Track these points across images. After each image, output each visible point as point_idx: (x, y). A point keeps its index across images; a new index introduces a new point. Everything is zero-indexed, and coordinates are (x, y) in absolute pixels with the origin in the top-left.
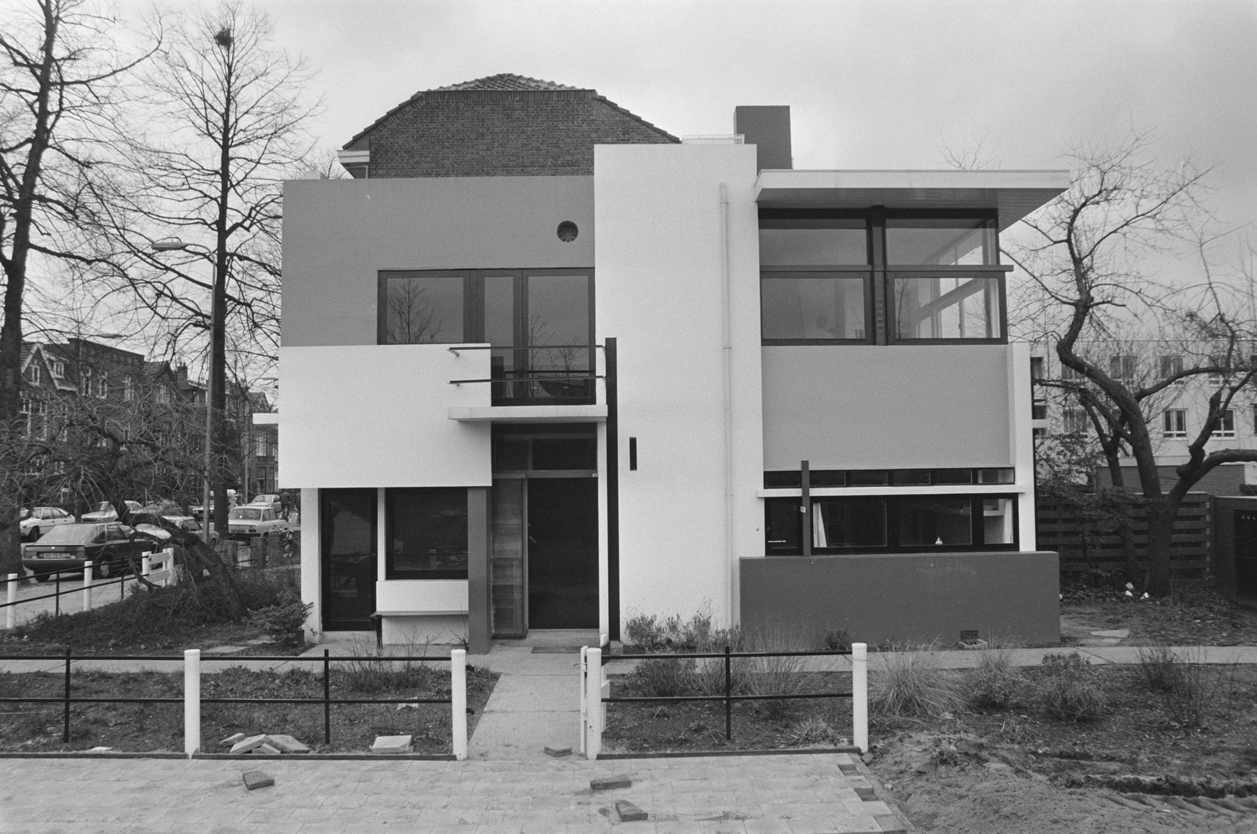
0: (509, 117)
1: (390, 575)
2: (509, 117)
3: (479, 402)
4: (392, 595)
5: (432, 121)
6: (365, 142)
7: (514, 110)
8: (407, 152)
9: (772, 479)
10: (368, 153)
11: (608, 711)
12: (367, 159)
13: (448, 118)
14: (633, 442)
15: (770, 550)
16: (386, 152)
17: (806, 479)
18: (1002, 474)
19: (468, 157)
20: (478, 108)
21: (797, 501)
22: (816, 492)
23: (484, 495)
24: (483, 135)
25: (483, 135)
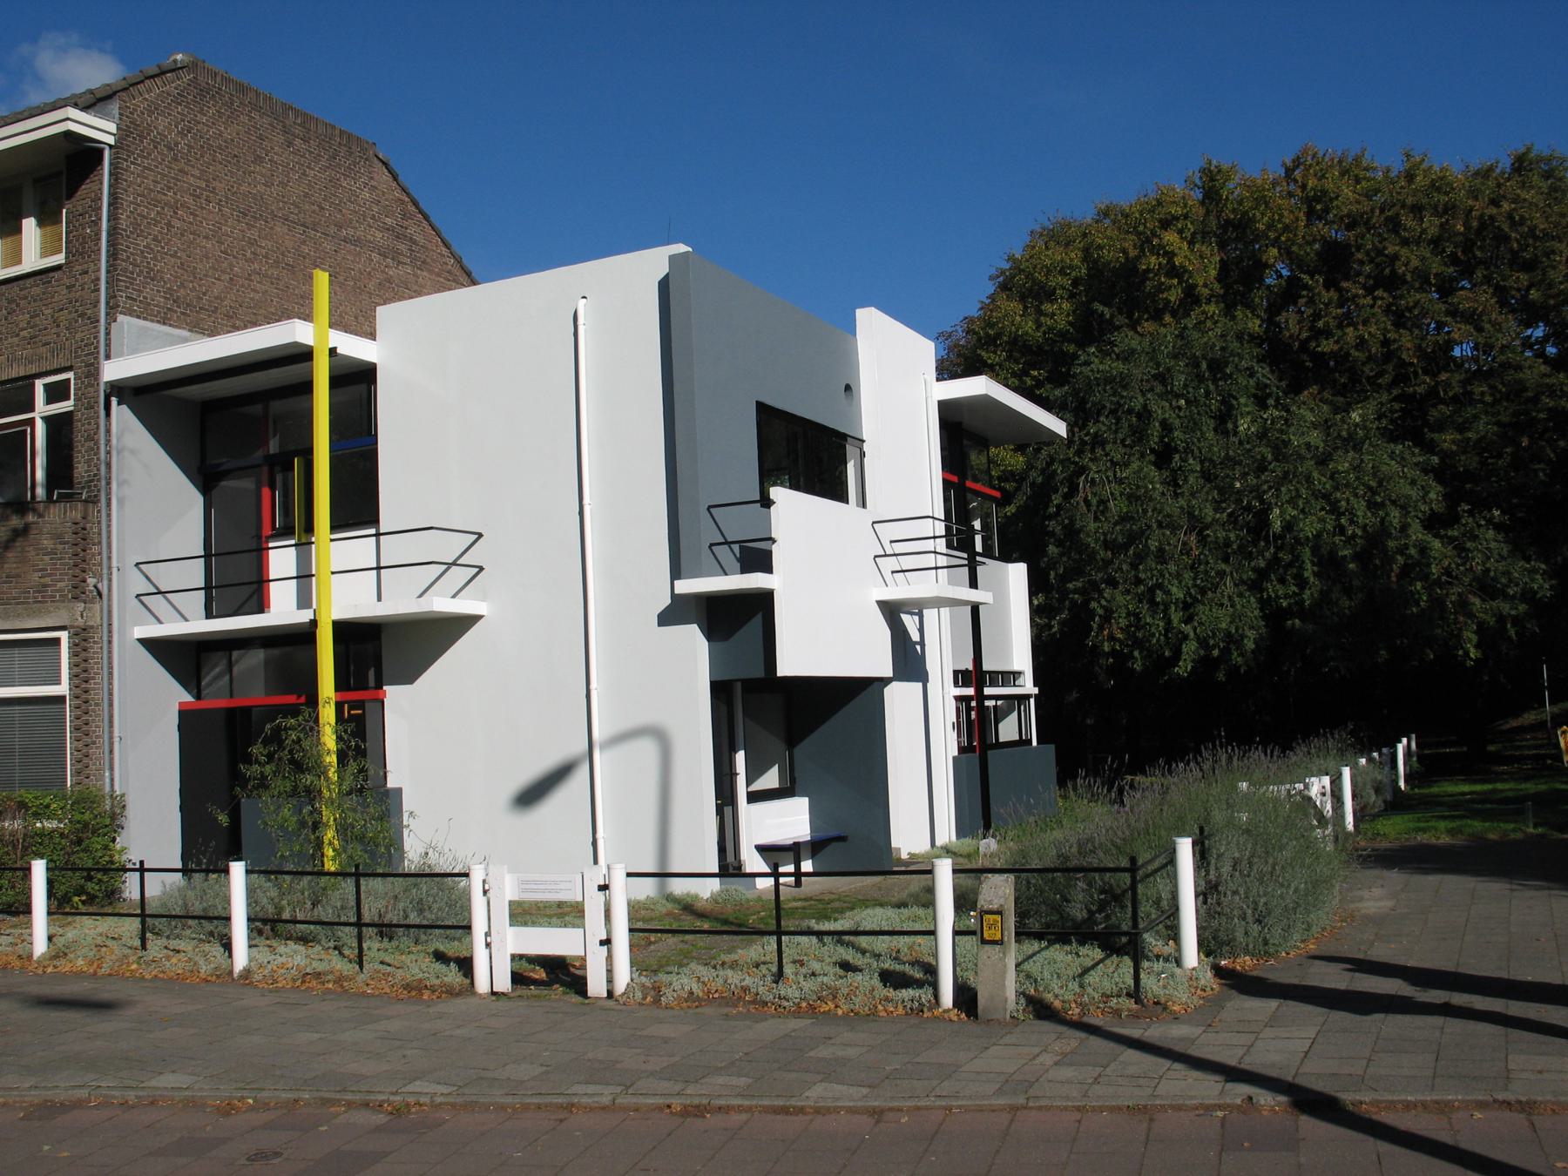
0: (290, 144)
6: (114, 107)
10: (112, 128)
12: (111, 140)
16: (142, 137)
18: (1011, 677)
19: (244, 188)
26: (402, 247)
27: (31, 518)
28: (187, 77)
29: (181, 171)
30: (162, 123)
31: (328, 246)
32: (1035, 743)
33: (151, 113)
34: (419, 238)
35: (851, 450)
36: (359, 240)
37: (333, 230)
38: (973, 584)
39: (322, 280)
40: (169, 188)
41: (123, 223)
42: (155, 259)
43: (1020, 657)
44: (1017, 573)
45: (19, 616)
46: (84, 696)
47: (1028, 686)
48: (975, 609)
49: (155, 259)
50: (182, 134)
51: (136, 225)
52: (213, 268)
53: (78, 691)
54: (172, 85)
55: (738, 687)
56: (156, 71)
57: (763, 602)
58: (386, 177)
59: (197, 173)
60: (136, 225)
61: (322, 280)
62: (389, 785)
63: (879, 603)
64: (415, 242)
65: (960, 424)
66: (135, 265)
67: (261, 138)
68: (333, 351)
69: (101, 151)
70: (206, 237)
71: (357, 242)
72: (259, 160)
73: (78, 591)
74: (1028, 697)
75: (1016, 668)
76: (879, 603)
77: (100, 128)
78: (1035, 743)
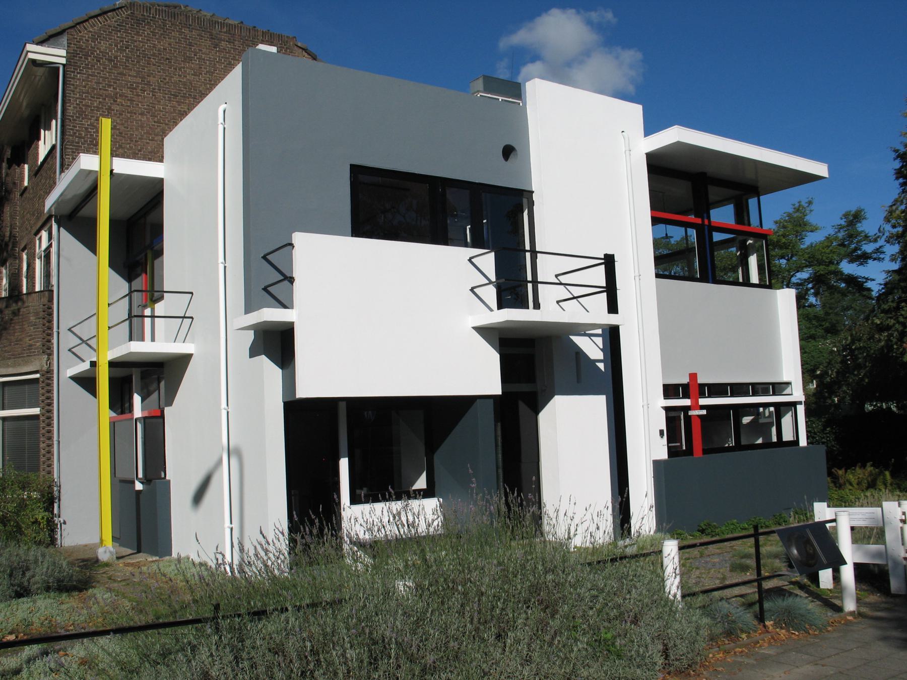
1: (355, 500)
4: (360, 519)
5: (138, 34)
6: (64, 40)
7: (221, 40)
8: (110, 60)
9: (670, 391)
10: (63, 53)
12: (63, 61)
13: (154, 34)
15: (672, 452)
17: (694, 391)
19: (175, 79)
21: (686, 409)
22: (703, 401)
23: (492, 401)
24: (190, 59)
25: (190, 59)
27: (20, 304)
28: (125, 14)
29: (121, 74)
30: (103, 45)
32: (803, 442)
33: (94, 40)
35: (525, 201)
38: (613, 308)
39: (106, 124)
40: (110, 86)
41: (71, 110)
43: (789, 368)
44: (785, 300)
45: (19, 365)
46: (48, 414)
47: (797, 393)
50: (121, 50)
51: (81, 112)
52: (148, 133)
53: (44, 411)
54: (112, 20)
55: (343, 406)
56: (97, 12)
60: (81, 112)
61: (106, 124)
63: (474, 328)
66: (80, 137)
67: (190, 45)
69: (58, 68)
70: (142, 114)
73: (45, 348)
74: (794, 404)
75: (785, 379)
76: (474, 328)
77: (56, 54)
78: (803, 442)
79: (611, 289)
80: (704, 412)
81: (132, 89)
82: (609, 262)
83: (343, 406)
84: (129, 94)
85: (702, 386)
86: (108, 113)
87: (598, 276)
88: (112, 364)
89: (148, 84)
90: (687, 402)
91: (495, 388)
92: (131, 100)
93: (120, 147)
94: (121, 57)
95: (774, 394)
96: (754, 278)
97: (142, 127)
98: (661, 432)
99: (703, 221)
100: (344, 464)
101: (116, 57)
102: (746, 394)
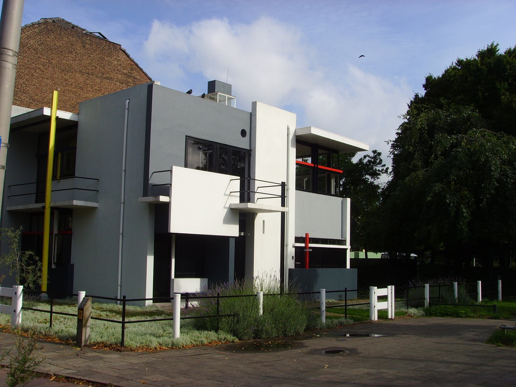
0: (84, 47)
2: (84, 47)
3: (235, 200)
5: (48, 37)
9: (298, 240)
11: (369, 316)
14: (264, 221)
19: (64, 62)
20: (70, 37)
22: (311, 245)
26: (130, 80)
30: (32, 42)
31: (98, 81)
34: (138, 77)
36: (111, 78)
37: (100, 75)
38: (283, 205)
40: (33, 63)
42: (26, 86)
48: (283, 214)
49: (26, 86)
50: (40, 45)
57: (167, 206)
58: (125, 57)
59: (45, 57)
62: (71, 263)
64: (136, 78)
65: (317, 144)
68: (57, 118)
71: (111, 79)
72: (71, 52)
79: (283, 197)
80: (311, 250)
81: (44, 65)
82: (283, 185)
83: (174, 237)
84: (42, 68)
85: (310, 238)
86: (57, 90)
87: (278, 191)
88: (53, 209)
89: (51, 63)
90: (303, 245)
91: (237, 234)
92: (43, 72)
93: (37, 95)
94: (40, 48)
95: (338, 244)
96: (333, 192)
97: (47, 85)
98: (293, 257)
99: (315, 165)
100: (173, 261)
101: (37, 48)
102: (327, 243)
